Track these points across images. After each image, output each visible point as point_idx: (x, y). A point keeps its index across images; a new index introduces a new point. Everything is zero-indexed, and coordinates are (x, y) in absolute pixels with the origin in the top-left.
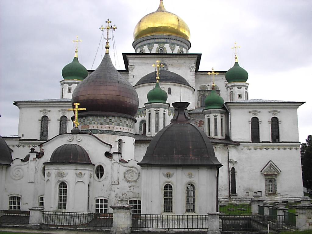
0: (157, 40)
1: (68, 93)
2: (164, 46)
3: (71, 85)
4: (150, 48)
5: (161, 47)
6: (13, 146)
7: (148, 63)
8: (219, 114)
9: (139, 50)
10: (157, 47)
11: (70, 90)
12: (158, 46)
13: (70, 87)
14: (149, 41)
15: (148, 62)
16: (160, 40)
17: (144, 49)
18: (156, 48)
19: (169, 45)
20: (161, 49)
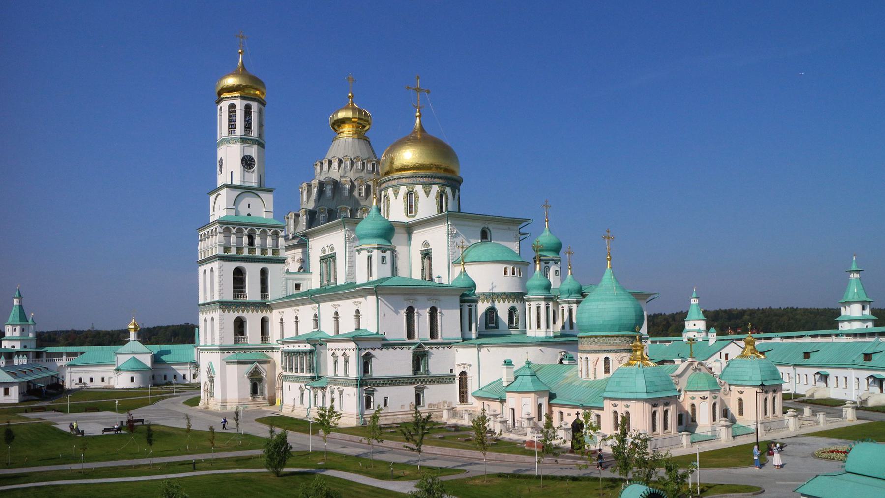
0: (437, 181)
1: (382, 263)
2: (446, 190)
3: (385, 252)
4: (427, 190)
6: (374, 349)
8: (575, 305)
9: (406, 189)
10: (438, 191)
11: (383, 258)
12: (439, 189)
13: (384, 255)
14: (425, 180)
16: (440, 181)
17: (416, 190)
18: (436, 191)
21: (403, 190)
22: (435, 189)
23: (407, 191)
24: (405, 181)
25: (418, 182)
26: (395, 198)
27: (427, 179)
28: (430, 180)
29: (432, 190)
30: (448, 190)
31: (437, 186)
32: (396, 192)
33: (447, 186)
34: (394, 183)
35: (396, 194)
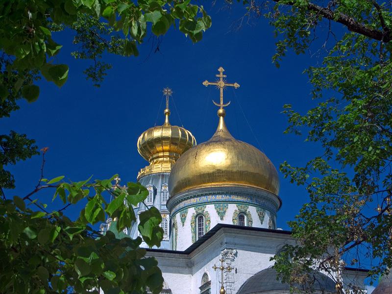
0: (235, 198)
2: (248, 210)
5: (243, 210)
7: (259, 247)
9: (194, 211)
12: (237, 209)
14: (219, 197)
15: (260, 245)
16: (240, 199)
19: (255, 208)
20: (241, 216)
21: (191, 212)
22: (232, 209)
23: (195, 213)
24: (193, 201)
25: (209, 200)
26: (182, 224)
27: (220, 196)
28: (227, 198)
29: (227, 210)
30: (252, 210)
31: (235, 205)
32: (184, 217)
33: (249, 204)
34: (182, 205)
35: (183, 220)
